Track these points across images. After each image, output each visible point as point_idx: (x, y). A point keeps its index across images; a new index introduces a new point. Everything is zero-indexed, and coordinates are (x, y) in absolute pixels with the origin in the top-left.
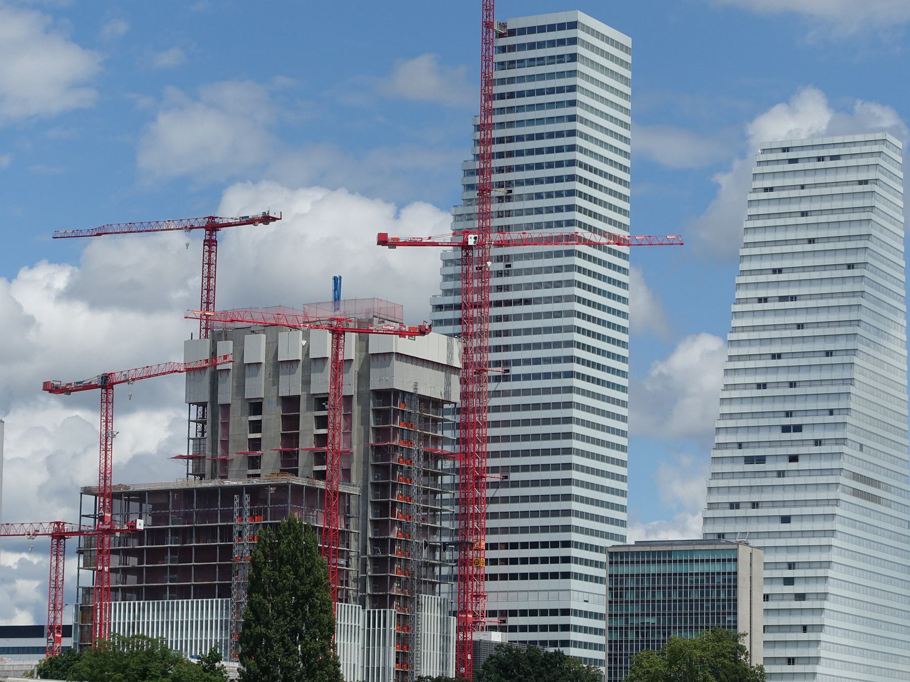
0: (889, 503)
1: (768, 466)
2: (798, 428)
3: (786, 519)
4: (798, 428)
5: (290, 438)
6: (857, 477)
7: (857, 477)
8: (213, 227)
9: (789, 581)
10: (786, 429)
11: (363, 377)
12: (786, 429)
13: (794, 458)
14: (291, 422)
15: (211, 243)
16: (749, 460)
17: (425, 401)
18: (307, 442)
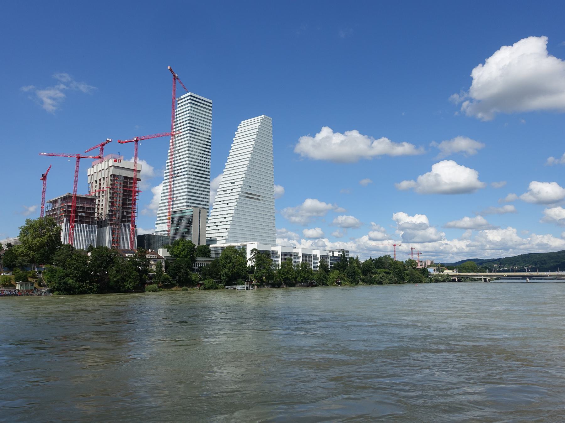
0: (264, 201)
1: (228, 192)
2: (234, 183)
3: (228, 204)
4: (234, 183)
5: (100, 188)
6: (246, 193)
7: (246, 193)
8: (103, 145)
9: (225, 218)
10: (232, 183)
11: (109, 172)
12: (232, 183)
13: (232, 190)
14: (100, 184)
15: (102, 149)
16: (224, 191)
17: (125, 178)
18: (102, 189)
